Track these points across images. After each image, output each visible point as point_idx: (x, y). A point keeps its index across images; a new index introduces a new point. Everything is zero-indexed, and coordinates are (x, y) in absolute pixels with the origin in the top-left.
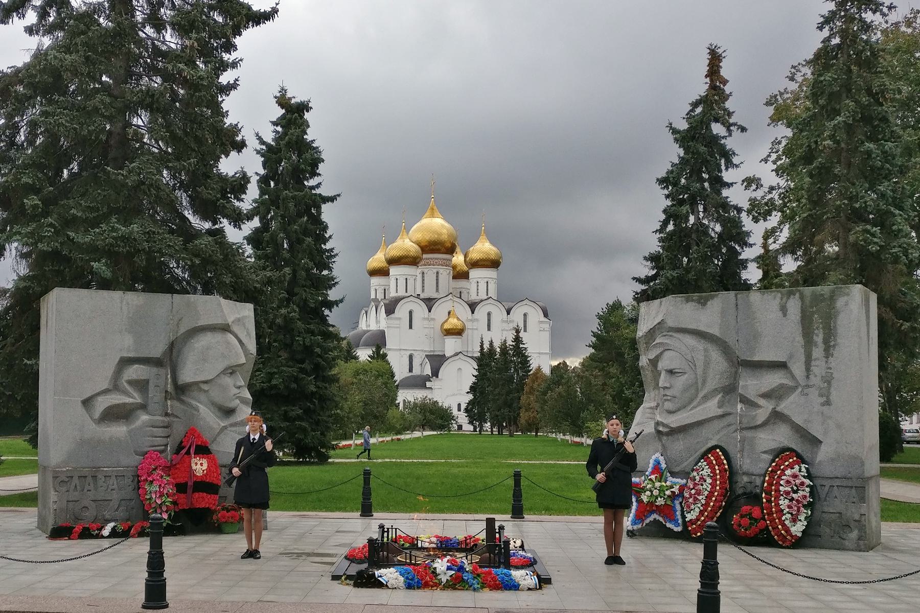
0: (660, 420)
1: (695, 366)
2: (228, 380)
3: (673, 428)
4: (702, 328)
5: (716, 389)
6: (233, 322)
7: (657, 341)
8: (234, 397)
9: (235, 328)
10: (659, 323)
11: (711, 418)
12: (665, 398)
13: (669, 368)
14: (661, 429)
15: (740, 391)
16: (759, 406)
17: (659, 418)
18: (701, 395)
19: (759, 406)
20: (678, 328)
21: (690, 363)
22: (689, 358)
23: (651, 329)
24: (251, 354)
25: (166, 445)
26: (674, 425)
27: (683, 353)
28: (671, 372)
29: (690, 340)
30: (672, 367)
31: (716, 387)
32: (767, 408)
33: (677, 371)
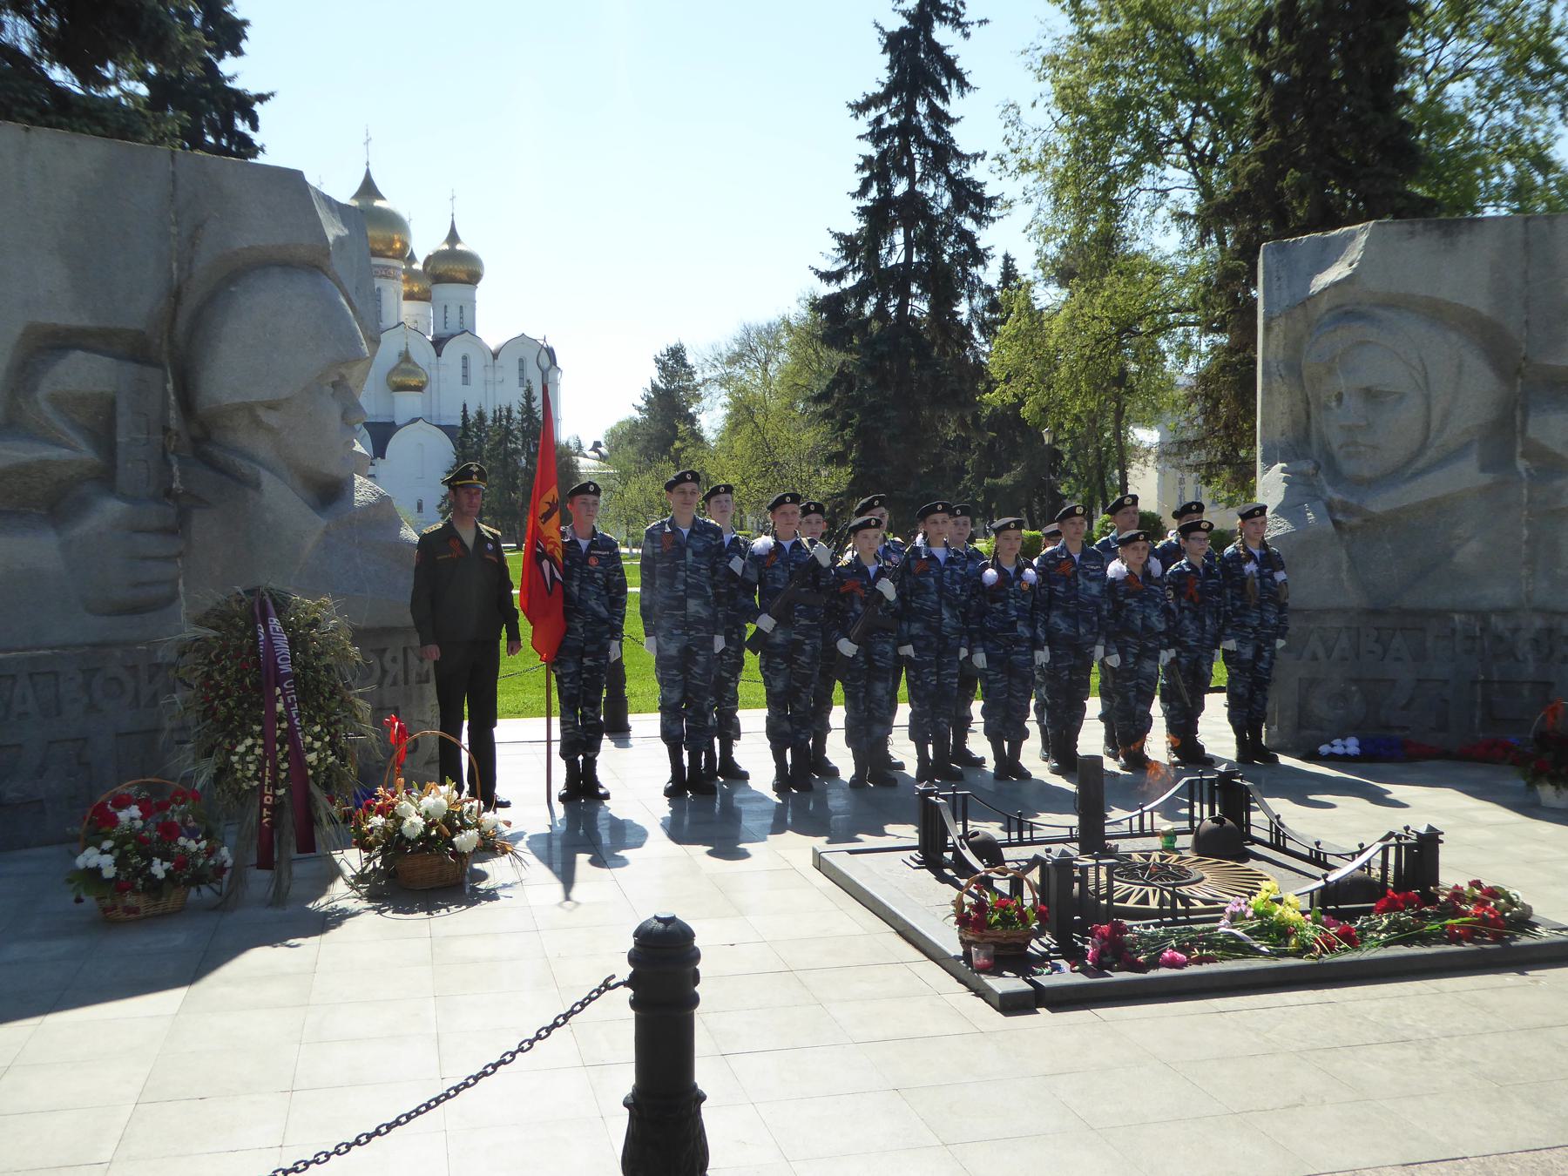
1: (1426, 377)
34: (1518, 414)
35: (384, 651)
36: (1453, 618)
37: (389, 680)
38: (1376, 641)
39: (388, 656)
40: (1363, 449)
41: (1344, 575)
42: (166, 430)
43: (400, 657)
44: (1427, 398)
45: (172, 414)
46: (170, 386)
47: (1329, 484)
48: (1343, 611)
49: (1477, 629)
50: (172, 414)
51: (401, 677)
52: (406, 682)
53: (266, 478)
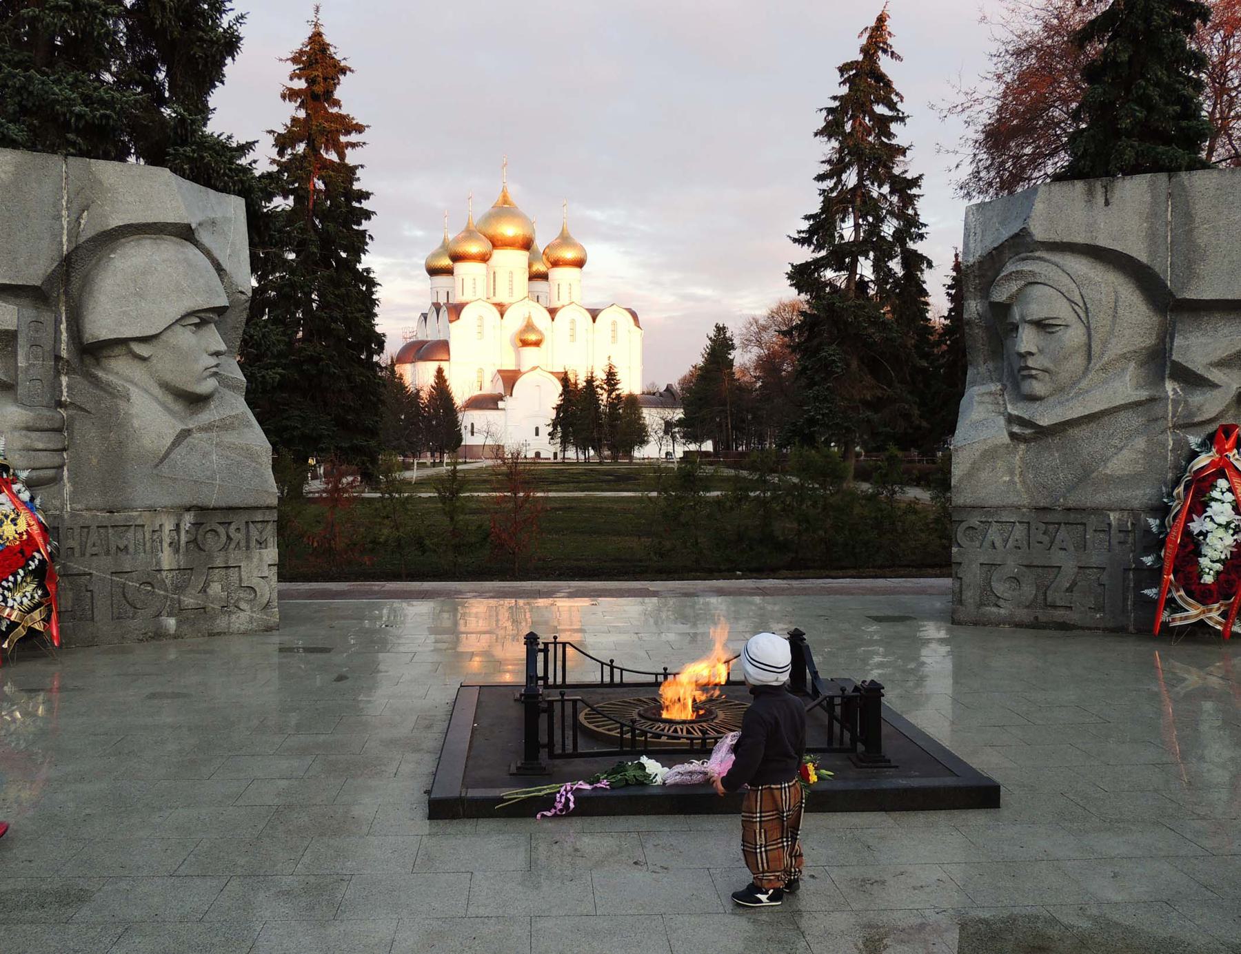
0: (1016, 413)
1: (1087, 311)
2: (185, 338)
3: (1042, 427)
4: (1103, 241)
5: (1124, 356)
6: (200, 224)
7: (1010, 268)
8: (207, 373)
9: (204, 237)
10: (1016, 235)
11: (1115, 407)
12: (1025, 373)
13: (1035, 317)
14: (1016, 429)
15: (1174, 358)
16: (1214, 386)
17: (1011, 409)
18: (1096, 364)
19: (1214, 386)
20: (1055, 243)
21: (1076, 307)
22: (1077, 299)
23: (995, 249)
24: (242, 292)
25: (61, 467)
26: (1044, 421)
27: (1064, 290)
28: (1042, 325)
29: (1079, 266)
30: (1042, 316)
31: (1125, 350)
32: (1229, 386)
33: (1051, 322)
34: (1168, 339)
35: (230, 523)
36: (1109, 516)
37: (232, 546)
38: (1044, 533)
39: (233, 527)
40: (1034, 372)
41: (1016, 479)
42: (58, 358)
43: (243, 531)
44: (1088, 328)
45: (63, 346)
46: (63, 327)
47: (1010, 402)
48: (1018, 508)
49: (1129, 524)
50: (63, 346)
51: (243, 544)
52: (248, 548)
53: (135, 393)
